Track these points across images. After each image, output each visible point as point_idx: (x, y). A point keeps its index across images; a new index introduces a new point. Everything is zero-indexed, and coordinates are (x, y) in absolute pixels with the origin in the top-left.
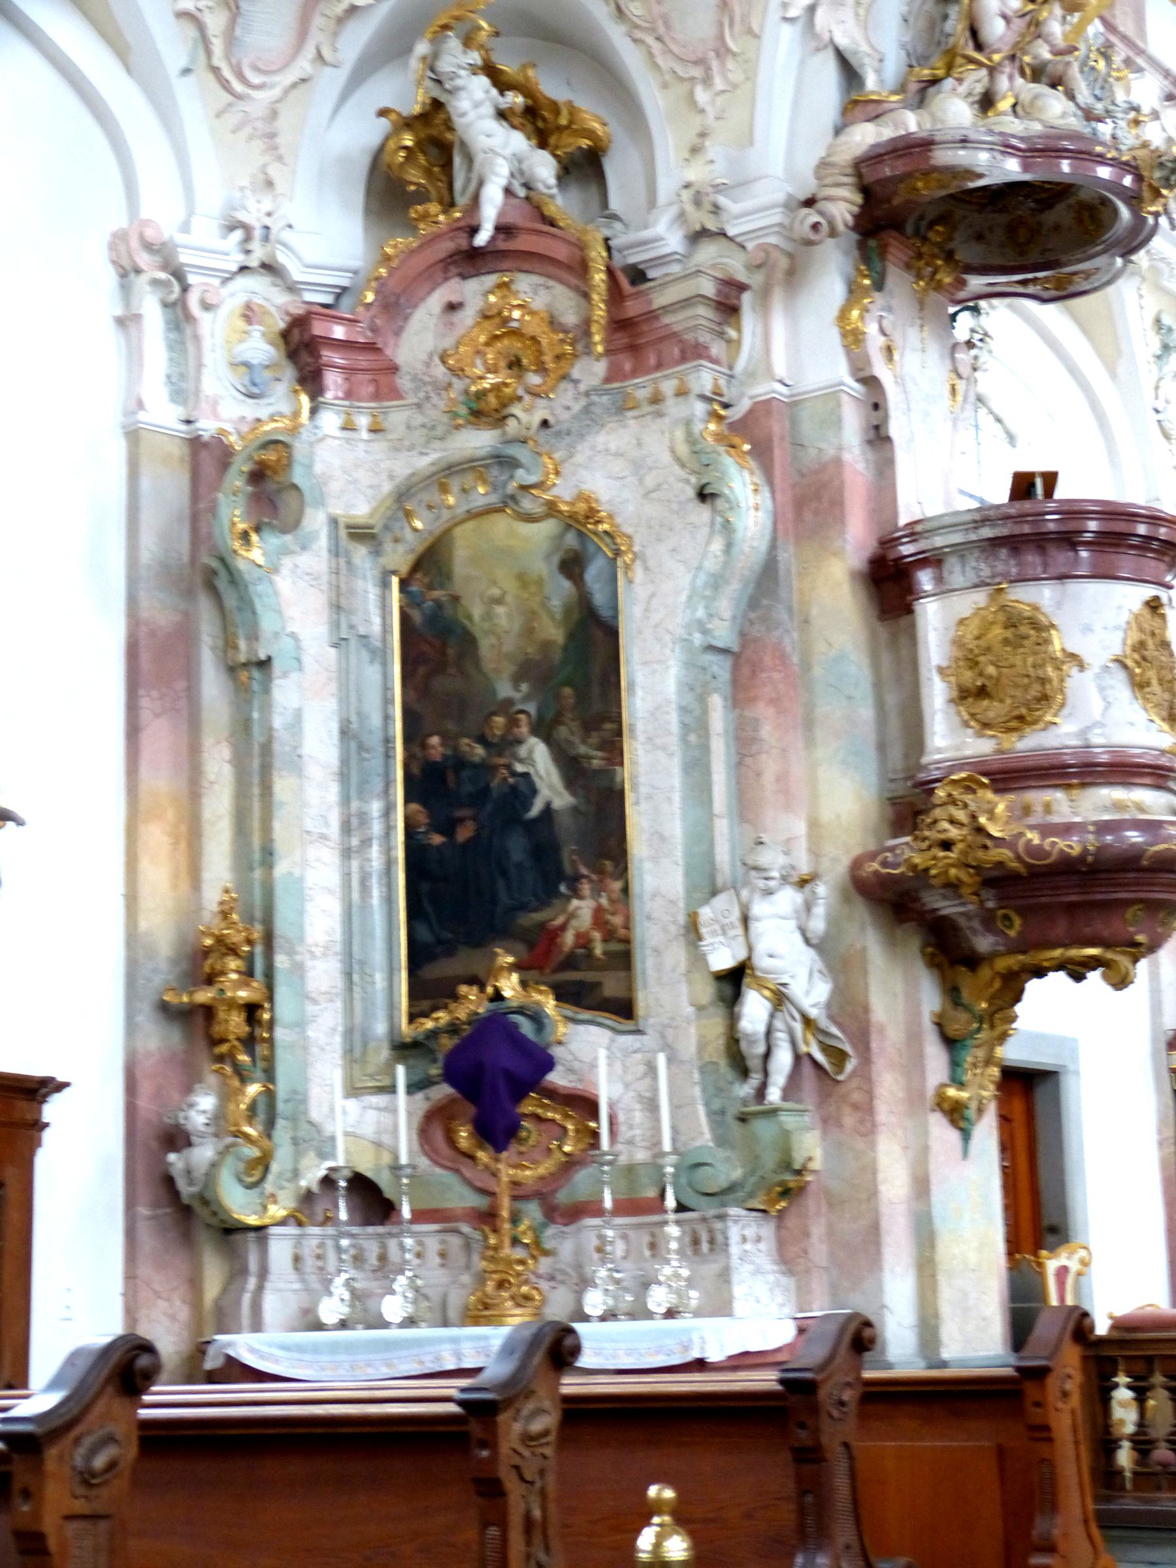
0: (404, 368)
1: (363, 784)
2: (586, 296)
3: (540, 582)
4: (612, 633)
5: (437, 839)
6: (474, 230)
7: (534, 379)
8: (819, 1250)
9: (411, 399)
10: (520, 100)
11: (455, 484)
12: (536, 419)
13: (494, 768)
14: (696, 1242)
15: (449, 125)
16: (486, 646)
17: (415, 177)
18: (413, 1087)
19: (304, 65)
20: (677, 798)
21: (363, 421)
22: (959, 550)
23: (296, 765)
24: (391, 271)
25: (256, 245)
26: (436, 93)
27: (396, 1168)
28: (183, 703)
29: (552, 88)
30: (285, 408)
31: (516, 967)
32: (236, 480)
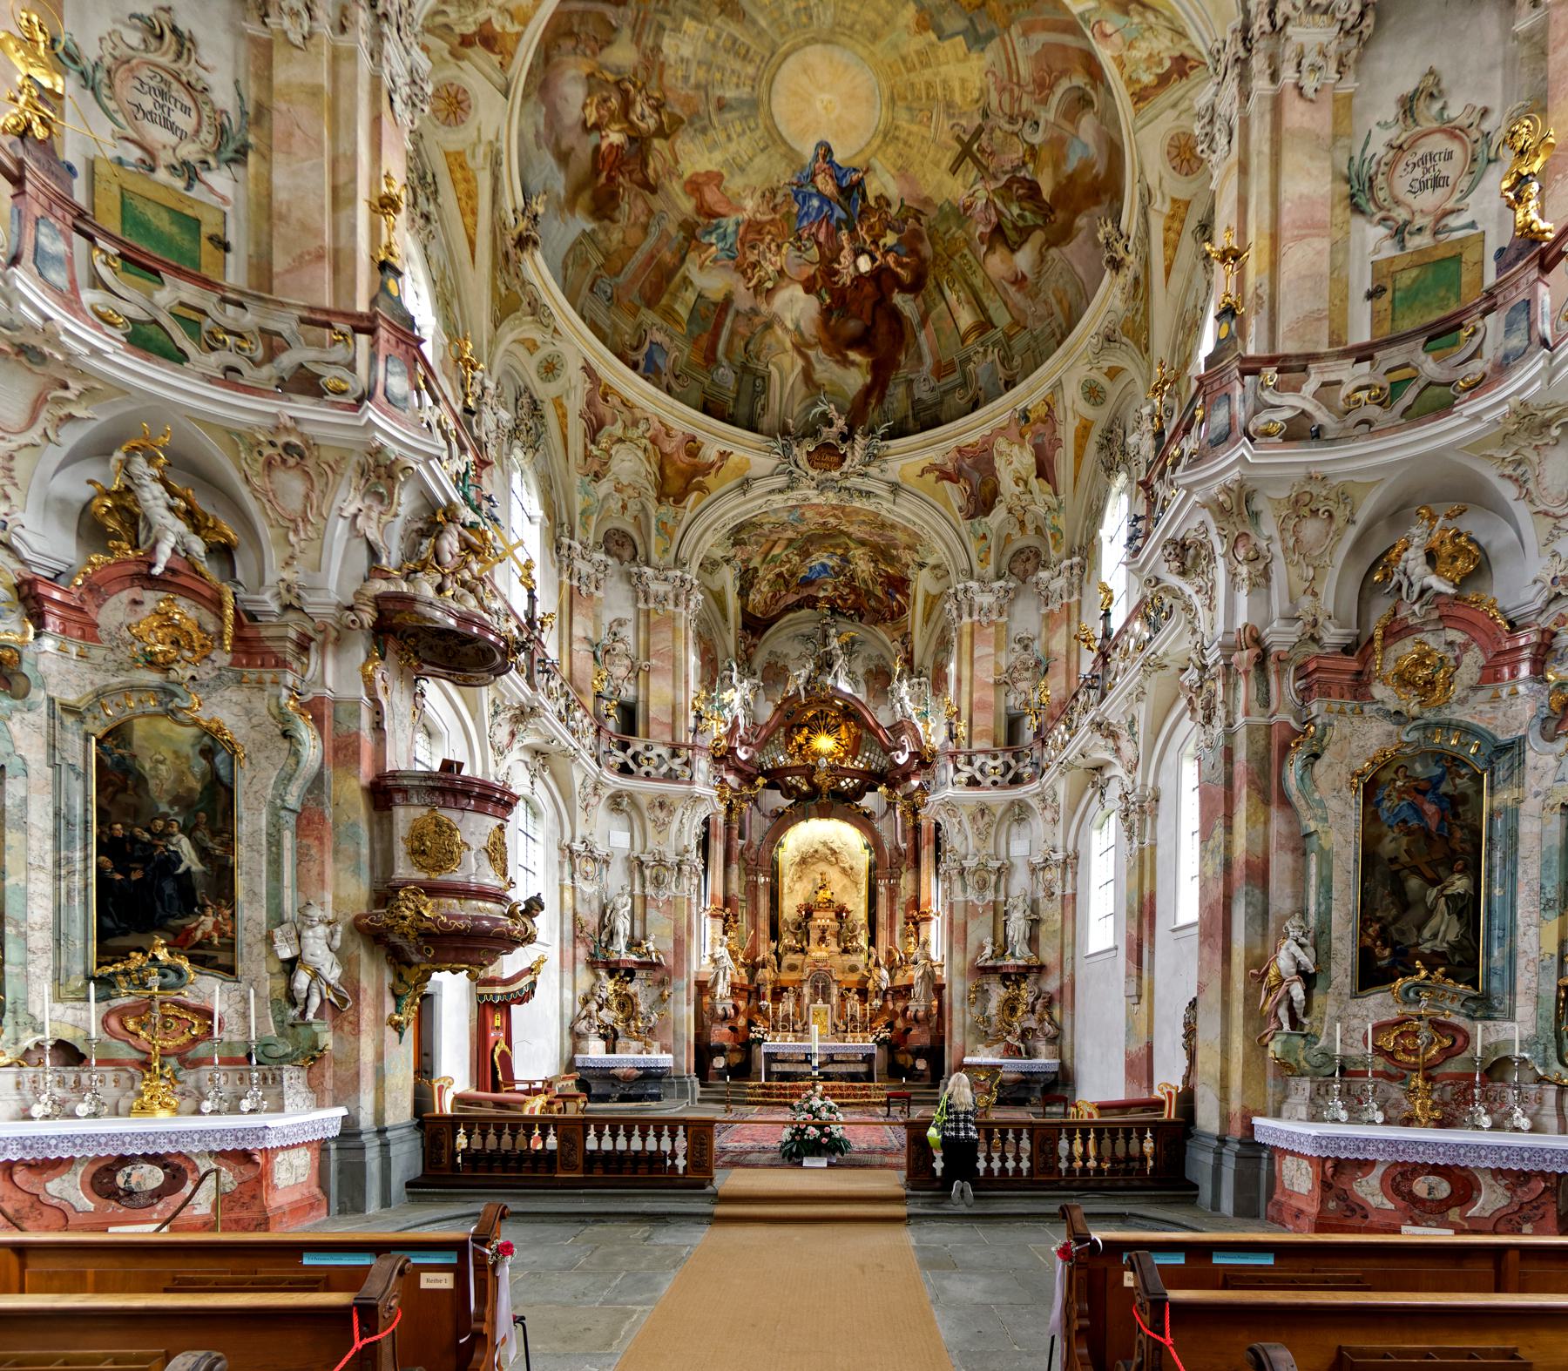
0: (103, 627)
1: (70, 844)
2: (221, 619)
3: (187, 757)
4: (230, 791)
5: (118, 877)
6: (152, 565)
7: (188, 654)
8: (329, 1083)
9: (106, 644)
10: (183, 504)
11: (135, 696)
12: (189, 674)
13: (156, 846)
14: (265, 1079)
15: (136, 502)
16: (152, 784)
17: (112, 524)
18: (97, 1000)
19: (34, 435)
20: (264, 875)
21: (74, 650)
22: (417, 788)
23: (23, 826)
24: (95, 571)
26: (128, 483)
27: (88, 1040)
29: (203, 504)
30: (18, 629)
31: (167, 945)
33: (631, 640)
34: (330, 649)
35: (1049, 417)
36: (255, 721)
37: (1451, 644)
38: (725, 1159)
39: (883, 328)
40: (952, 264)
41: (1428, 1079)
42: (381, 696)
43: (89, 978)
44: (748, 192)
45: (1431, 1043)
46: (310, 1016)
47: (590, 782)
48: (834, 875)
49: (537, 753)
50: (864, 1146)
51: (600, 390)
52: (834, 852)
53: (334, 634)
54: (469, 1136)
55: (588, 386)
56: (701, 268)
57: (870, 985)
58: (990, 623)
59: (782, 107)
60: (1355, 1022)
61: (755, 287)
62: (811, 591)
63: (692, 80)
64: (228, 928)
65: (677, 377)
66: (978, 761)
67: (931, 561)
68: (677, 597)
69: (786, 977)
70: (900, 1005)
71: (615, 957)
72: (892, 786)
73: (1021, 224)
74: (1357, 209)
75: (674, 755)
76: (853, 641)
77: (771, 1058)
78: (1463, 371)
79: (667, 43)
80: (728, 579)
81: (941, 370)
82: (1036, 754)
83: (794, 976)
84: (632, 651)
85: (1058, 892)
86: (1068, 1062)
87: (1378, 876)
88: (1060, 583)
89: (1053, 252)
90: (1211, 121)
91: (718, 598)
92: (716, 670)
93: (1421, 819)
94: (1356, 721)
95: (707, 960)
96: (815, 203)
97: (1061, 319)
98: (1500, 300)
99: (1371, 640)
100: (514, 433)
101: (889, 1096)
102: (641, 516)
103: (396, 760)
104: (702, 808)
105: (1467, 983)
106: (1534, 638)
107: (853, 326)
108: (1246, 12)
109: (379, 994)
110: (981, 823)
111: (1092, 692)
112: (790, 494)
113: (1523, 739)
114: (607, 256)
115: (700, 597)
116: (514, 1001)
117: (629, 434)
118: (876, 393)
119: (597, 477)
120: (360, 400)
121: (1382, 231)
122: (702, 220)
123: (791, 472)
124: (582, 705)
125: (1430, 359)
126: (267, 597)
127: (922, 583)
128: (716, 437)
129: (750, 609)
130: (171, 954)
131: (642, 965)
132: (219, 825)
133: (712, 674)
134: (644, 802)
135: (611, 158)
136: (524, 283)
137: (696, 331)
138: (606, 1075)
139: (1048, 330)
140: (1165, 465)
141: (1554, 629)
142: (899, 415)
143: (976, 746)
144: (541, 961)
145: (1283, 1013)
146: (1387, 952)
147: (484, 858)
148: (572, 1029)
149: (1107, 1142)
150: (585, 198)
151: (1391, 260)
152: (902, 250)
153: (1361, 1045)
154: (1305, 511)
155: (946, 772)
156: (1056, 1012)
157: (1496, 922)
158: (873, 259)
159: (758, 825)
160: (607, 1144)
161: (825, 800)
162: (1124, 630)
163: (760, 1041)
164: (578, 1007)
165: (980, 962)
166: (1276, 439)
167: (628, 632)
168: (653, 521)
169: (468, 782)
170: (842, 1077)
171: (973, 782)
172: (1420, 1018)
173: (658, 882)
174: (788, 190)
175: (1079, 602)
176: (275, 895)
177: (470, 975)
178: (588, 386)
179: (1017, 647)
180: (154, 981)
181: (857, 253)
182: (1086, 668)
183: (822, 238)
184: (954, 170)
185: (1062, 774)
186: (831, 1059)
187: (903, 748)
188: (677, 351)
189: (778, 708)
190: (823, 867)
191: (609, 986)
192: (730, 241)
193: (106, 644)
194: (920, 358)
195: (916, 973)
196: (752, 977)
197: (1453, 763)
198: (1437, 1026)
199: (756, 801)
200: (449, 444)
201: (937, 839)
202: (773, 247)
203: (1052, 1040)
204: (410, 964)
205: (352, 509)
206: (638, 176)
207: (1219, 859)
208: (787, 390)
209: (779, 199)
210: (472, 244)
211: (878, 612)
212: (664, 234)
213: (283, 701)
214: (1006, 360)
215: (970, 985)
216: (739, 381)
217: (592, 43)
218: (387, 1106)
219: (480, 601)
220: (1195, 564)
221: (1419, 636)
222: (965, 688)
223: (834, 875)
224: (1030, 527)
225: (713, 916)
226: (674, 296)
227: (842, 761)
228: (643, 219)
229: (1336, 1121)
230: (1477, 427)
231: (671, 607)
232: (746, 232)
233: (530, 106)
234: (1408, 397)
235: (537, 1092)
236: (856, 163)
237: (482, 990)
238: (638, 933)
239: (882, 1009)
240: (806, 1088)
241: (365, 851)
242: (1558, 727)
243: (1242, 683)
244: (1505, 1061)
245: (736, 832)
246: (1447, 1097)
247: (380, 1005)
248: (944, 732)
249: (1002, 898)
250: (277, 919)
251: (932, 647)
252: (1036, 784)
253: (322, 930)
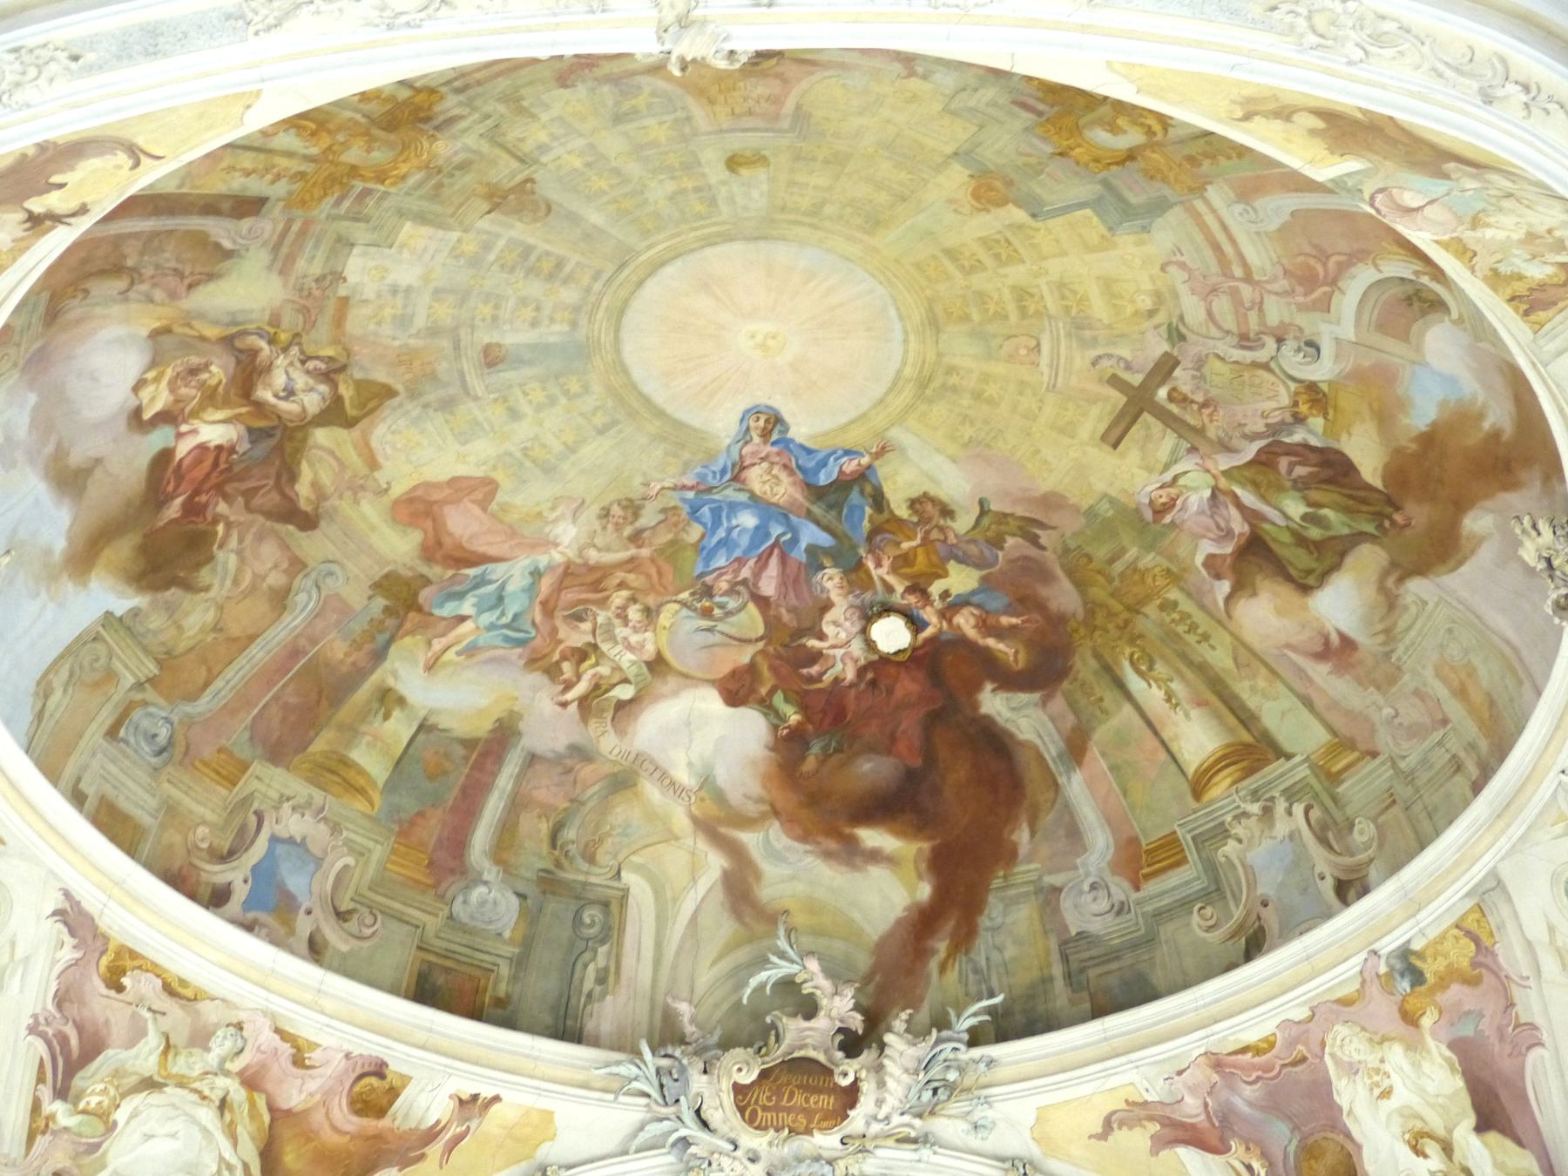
40: (1140, 624)
56: (430, 667)
61: (584, 702)
73: (1315, 533)
96: (748, 520)
97: (1471, 730)
117: (179, 1066)
118: (949, 926)
122: (435, 571)
123: (685, 1142)
142: (1023, 978)
152: (997, 601)
158: (916, 624)
174: (673, 500)
181: (868, 616)
184: (1114, 438)
192: (512, 608)
202: (634, 613)
212: (333, 606)
226: (351, 732)
228: (276, 579)
232: (559, 588)
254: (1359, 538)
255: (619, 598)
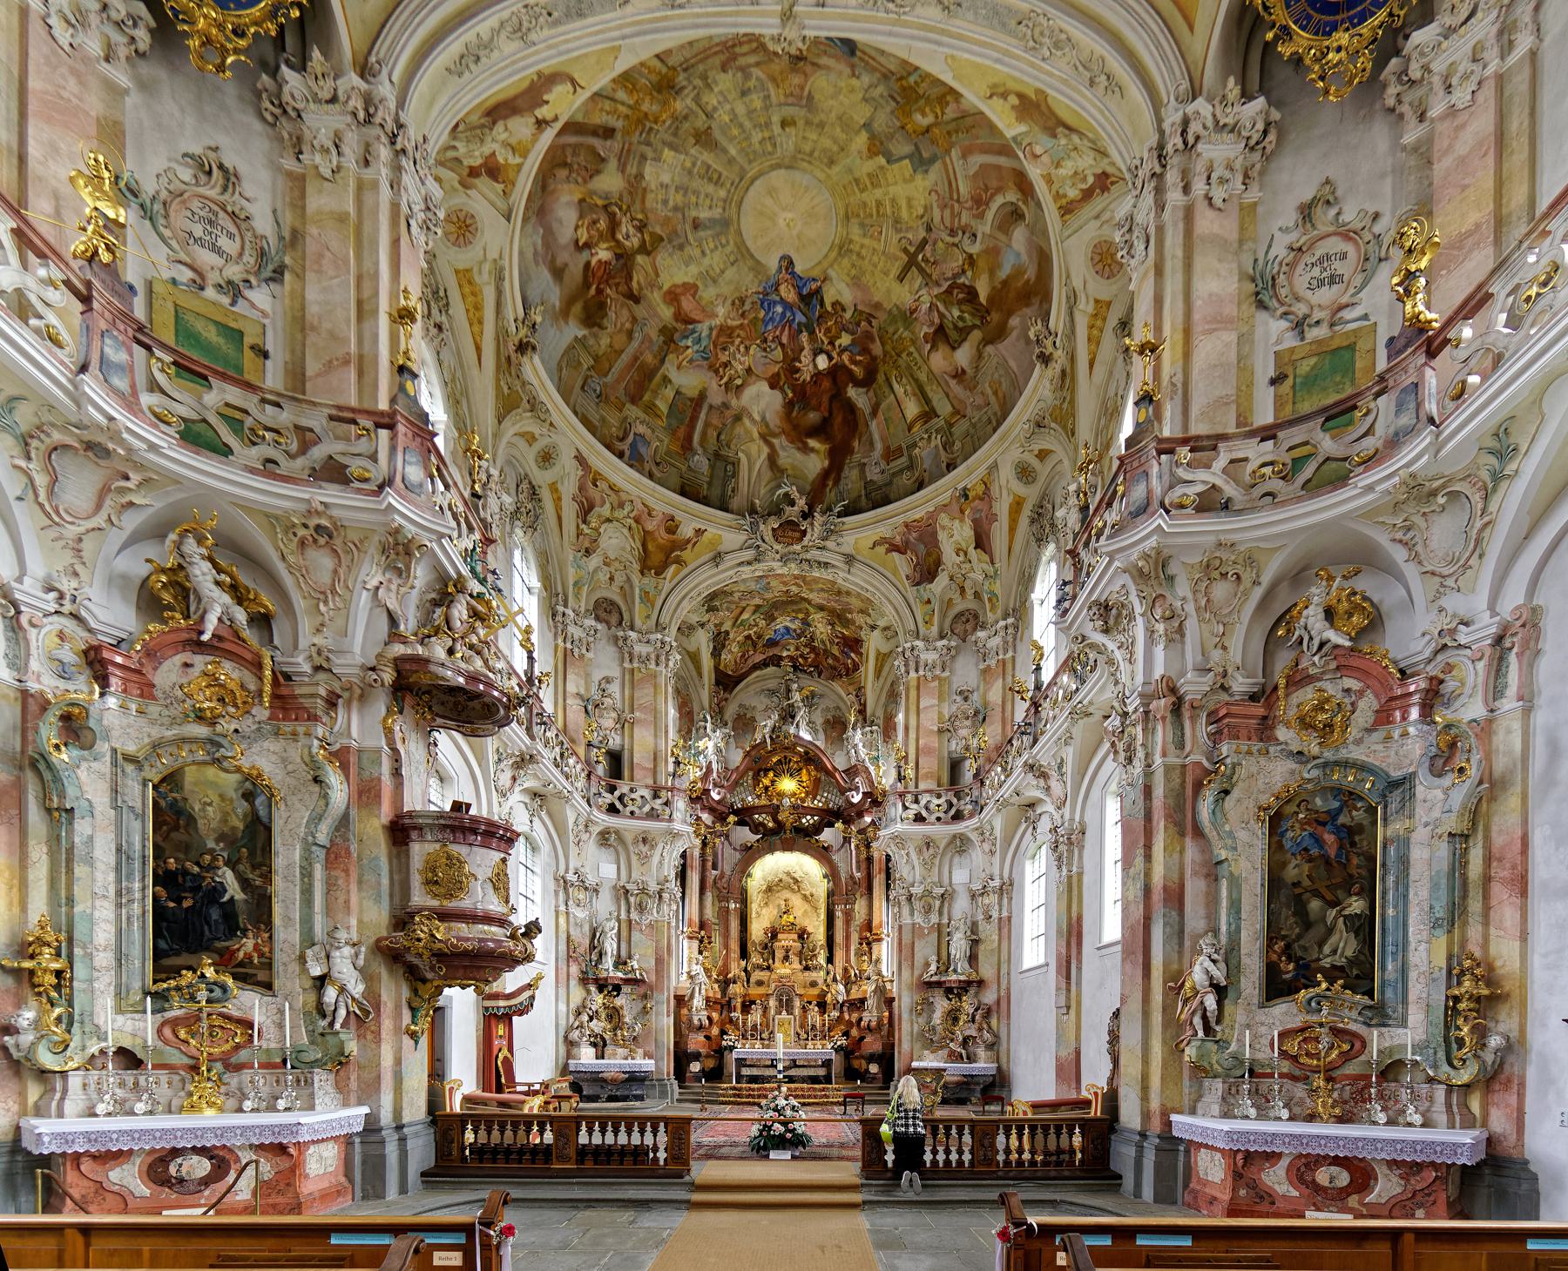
1: (130, 876)
3: (231, 800)
4: (269, 829)
5: (172, 905)
6: (201, 633)
7: (232, 710)
8: (353, 1085)
9: (162, 702)
11: (186, 747)
12: (232, 727)
14: (298, 1081)
15: (187, 577)
16: (201, 823)
17: (167, 597)
18: (153, 1012)
19: (99, 520)
21: (134, 707)
22: (431, 826)
23: (90, 861)
25: (67, 602)
27: (145, 1047)
28: (16, 821)
29: (245, 579)
30: (85, 689)
32: (52, 717)
33: (617, 695)
34: (355, 704)
35: (986, 496)
36: (290, 768)
37: (1348, 691)
38: (701, 1152)
39: (838, 419)
40: (901, 362)
41: (1329, 1079)
42: (399, 746)
43: (146, 993)
44: (720, 301)
45: (1332, 1047)
46: (337, 1026)
47: (582, 821)
48: (796, 901)
49: (535, 795)
50: (824, 1140)
51: (591, 476)
52: (796, 881)
53: (358, 691)
54: (476, 1132)
55: (580, 473)
57: (829, 998)
58: (935, 678)
59: (749, 225)
60: (1263, 1030)
62: (776, 651)
63: (671, 203)
64: (266, 950)
65: (658, 464)
66: (924, 799)
67: (882, 623)
68: (658, 657)
69: (755, 991)
70: (855, 1016)
71: (604, 974)
72: (847, 822)
73: (961, 324)
74: (1261, 305)
75: (656, 796)
76: (813, 695)
77: (741, 1063)
78: (1357, 447)
79: (649, 170)
80: (702, 641)
81: (890, 454)
82: (976, 793)
83: (761, 990)
84: (619, 705)
85: (995, 915)
86: (1004, 1066)
87: (1283, 899)
88: (995, 642)
89: (990, 349)
90: (1130, 230)
91: (694, 658)
92: (691, 721)
93: (1321, 847)
94: (1263, 761)
95: (685, 977)
96: (779, 309)
97: (996, 407)
98: (1391, 383)
99: (1276, 688)
100: (515, 514)
101: (846, 1097)
102: (627, 587)
103: (413, 801)
104: (680, 843)
105: (1363, 994)
106: (1423, 685)
107: (813, 417)
108: (1161, 132)
109: (398, 1008)
110: (926, 855)
111: (1025, 738)
112: (757, 566)
113: (1413, 775)
114: (596, 358)
115: (679, 657)
116: (515, 1013)
117: (616, 514)
119: (588, 552)
120: (381, 487)
121: (1284, 324)
122: (680, 326)
124: (574, 753)
125: (1328, 436)
126: (300, 659)
127: (874, 643)
128: (692, 517)
129: (721, 667)
130: (217, 972)
131: (627, 981)
132: (259, 859)
133: (689, 725)
134: (629, 838)
135: (600, 274)
136: (524, 384)
137: (674, 423)
138: (596, 1078)
139: (985, 419)
140: (1090, 536)
141: (1441, 676)
142: (854, 495)
143: (922, 786)
144: (540, 978)
145: (1197, 1021)
146: (1291, 966)
147: (489, 886)
148: (566, 1038)
149: (1040, 1136)
150: (577, 308)
151: (1292, 350)
152: (856, 350)
153: (1268, 1050)
154: (1216, 574)
155: (895, 809)
156: (994, 1022)
157: (1390, 939)
158: (830, 358)
159: (730, 857)
160: (597, 1139)
161: (788, 835)
162: (1053, 682)
163: (731, 1048)
164: (572, 1019)
165: (926, 977)
166: (1189, 511)
167: (615, 688)
168: (637, 591)
169: (475, 820)
170: (804, 1080)
171: (919, 819)
172: (1321, 1025)
173: (641, 908)
175: (1013, 658)
176: (307, 922)
177: (478, 991)
178: (580, 473)
179: (959, 699)
180: (202, 995)
181: (815, 355)
182: (1020, 716)
183: (785, 340)
184: (901, 278)
185: (999, 810)
186: (794, 1064)
187: (857, 789)
188: (659, 441)
189: (747, 754)
190: (786, 894)
191: (598, 1000)
192: (704, 343)
193: (162, 702)
194: (872, 444)
195: (869, 988)
196: (724, 991)
197: (1349, 797)
198: (1336, 1032)
199: (727, 837)
200: (459, 524)
201: (888, 869)
203: (991, 1047)
204: (424, 981)
205: (374, 583)
206: (624, 288)
207: (1140, 885)
208: (755, 473)
209: (747, 307)
210: (478, 349)
211: (834, 668)
212: (647, 339)
213: (314, 750)
214: (947, 446)
215: (917, 998)
216: (712, 467)
217: (583, 173)
218: (404, 1105)
219: (486, 662)
220: (1117, 623)
221: (1318, 684)
222: (912, 735)
223: (796, 901)
224: (969, 593)
225: (690, 938)
226: (655, 393)
227: (803, 800)
228: (628, 325)
229: (1247, 1117)
230: (1370, 497)
231: (652, 666)
232: (718, 336)
233: (529, 227)
234: (1308, 471)
235: (536, 1093)
236: (815, 273)
237: (488, 1003)
238: (624, 953)
239: (840, 1019)
240: (772, 1090)
241: (385, 881)
242: (1445, 764)
243: (1159, 728)
244: (1400, 1063)
245: (710, 864)
246: (1346, 1095)
247: (398, 1015)
248: (893, 774)
249: (945, 921)
250: (309, 941)
251: (883, 699)
252: (976, 820)
253: (347, 951)
254: (974, 327)
255: (737, 341)
